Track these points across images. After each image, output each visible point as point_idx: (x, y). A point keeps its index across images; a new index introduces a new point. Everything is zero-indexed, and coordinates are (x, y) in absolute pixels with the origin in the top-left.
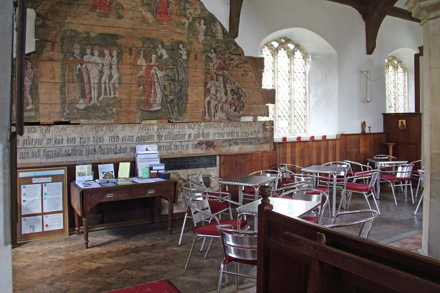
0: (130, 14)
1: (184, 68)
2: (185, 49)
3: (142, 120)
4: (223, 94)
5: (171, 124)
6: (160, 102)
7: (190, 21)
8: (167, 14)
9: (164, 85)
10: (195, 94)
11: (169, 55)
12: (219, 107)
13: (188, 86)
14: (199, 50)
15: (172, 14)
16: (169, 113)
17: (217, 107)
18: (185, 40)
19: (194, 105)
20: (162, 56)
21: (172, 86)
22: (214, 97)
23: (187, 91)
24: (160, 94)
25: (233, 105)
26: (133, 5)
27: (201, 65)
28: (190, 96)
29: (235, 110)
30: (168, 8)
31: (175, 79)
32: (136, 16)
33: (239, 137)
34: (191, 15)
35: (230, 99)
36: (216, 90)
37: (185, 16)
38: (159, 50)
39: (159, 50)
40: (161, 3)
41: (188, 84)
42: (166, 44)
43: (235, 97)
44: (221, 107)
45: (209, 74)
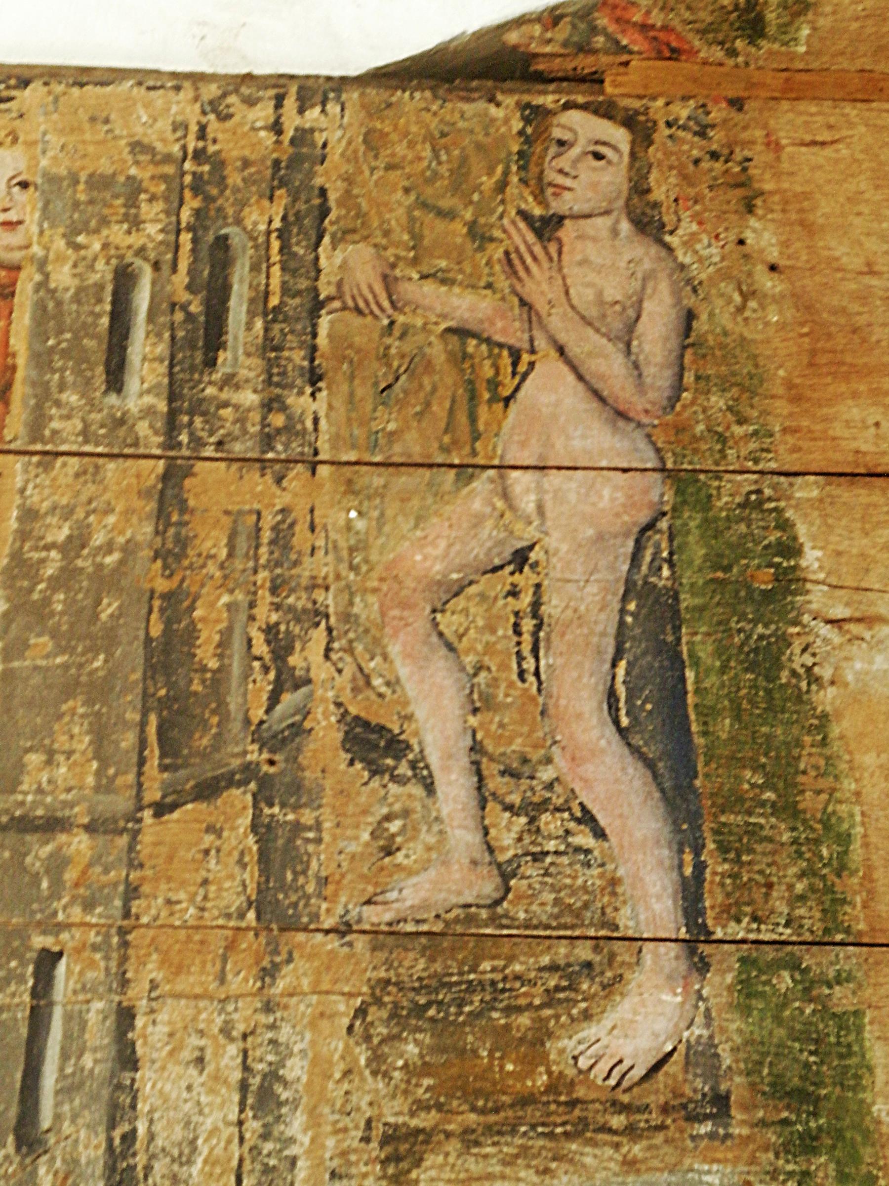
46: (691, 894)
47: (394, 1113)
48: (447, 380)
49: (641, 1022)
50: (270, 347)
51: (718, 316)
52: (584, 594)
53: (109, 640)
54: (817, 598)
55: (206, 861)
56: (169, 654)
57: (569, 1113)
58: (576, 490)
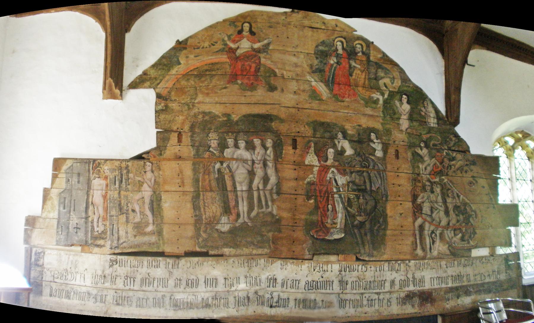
0: (293, 86)
1: (379, 171)
2: (379, 141)
3: (313, 255)
4: (442, 214)
5: (361, 262)
6: (343, 226)
8: (350, 86)
9: (349, 199)
10: (397, 212)
11: (355, 150)
12: (438, 235)
13: (387, 200)
14: (402, 143)
16: (357, 244)
17: (433, 235)
18: (378, 126)
19: (398, 232)
20: (343, 151)
21: (361, 200)
22: (429, 219)
23: (385, 208)
24: (342, 213)
25: (458, 232)
26: (298, 73)
27: (405, 167)
28: (391, 217)
29: (462, 239)
30: (351, 75)
31: (366, 189)
32: (302, 88)
33: (472, 283)
35: (453, 221)
36: (432, 207)
38: (339, 142)
39: (339, 142)
40: (340, 68)
41: (387, 197)
42: (349, 132)
43: (461, 217)
44: (441, 234)
45: (419, 181)
46: (153, 221)
47: (135, 234)
48: (138, 185)
49: (150, 228)
50: (126, 182)
51: (157, 179)
52: (147, 201)
53: (116, 204)
54: (163, 200)
55: (123, 218)
56: (120, 205)
57: (145, 234)
58: (147, 192)
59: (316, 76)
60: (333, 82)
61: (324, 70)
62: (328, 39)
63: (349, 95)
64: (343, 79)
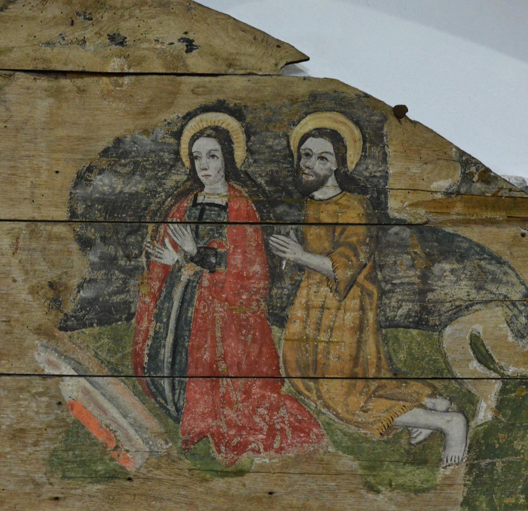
7: (485, 413)
15: (314, 373)
30: (282, 321)
34: (485, 358)
37: (439, 377)
40: (216, 290)
59: (87, 344)
60: (179, 372)
61: (127, 304)
62: (146, 132)
63: (272, 432)
64: (234, 347)
